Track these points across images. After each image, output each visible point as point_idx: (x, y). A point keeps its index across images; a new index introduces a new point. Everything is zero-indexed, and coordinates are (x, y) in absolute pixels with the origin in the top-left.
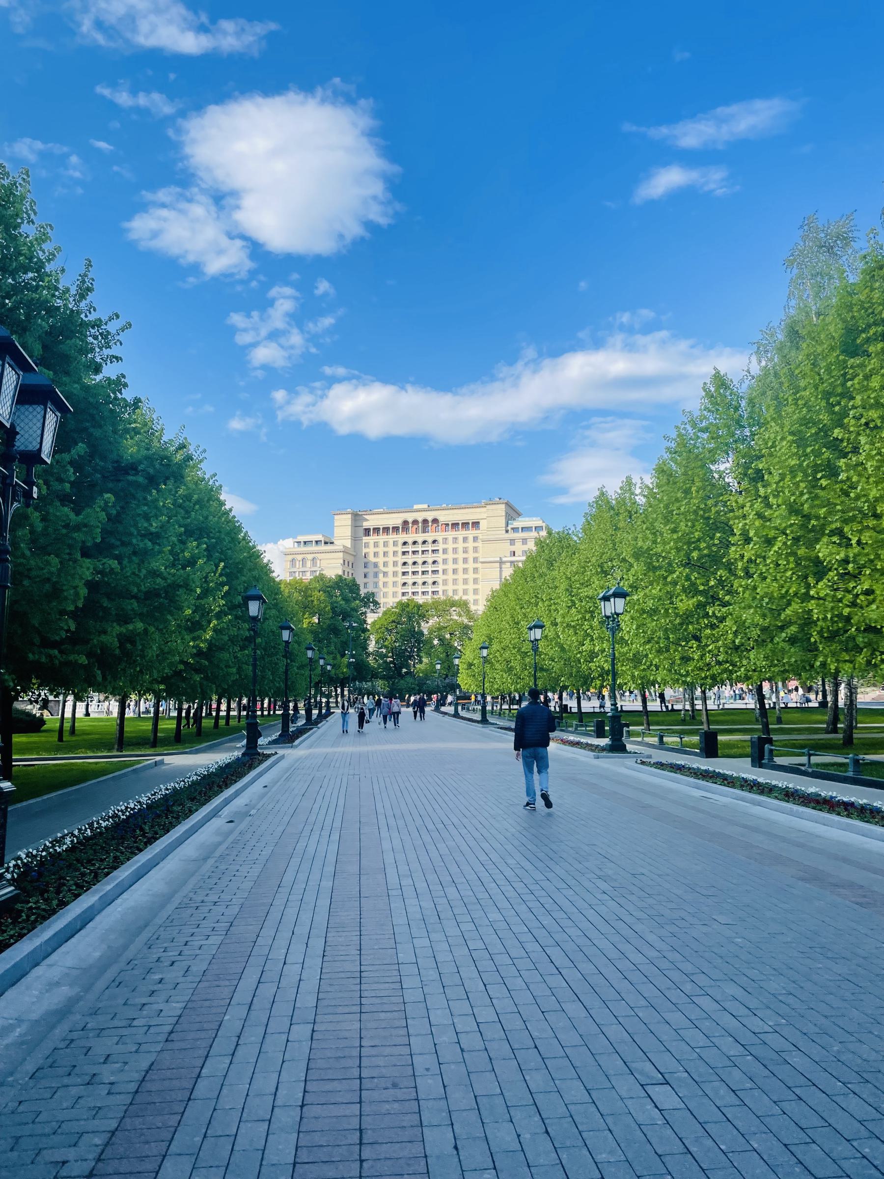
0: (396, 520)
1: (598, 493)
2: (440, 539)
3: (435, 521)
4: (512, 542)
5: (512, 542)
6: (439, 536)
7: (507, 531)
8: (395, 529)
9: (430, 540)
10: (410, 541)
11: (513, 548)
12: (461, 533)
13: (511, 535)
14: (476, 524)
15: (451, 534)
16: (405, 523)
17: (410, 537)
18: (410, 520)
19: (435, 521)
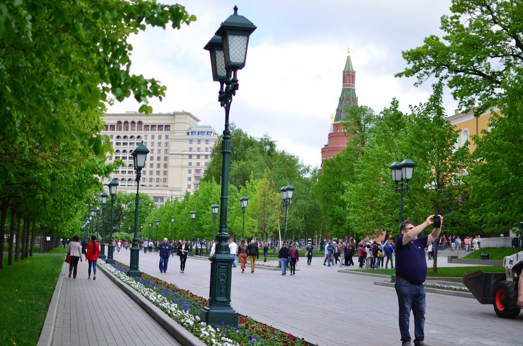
0: (114, 122)
1: (388, 106)
2: (143, 136)
3: (140, 123)
4: (191, 141)
5: (191, 141)
6: (142, 133)
7: (188, 134)
8: (112, 127)
9: (136, 136)
10: (122, 136)
11: (191, 146)
12: (156, 133)
13: (190, 137)
14: (167, 127)
15: (150, 133)
16: (119, 122)
17: (122, 133)
18: (123, 121)
19: (140, 123)
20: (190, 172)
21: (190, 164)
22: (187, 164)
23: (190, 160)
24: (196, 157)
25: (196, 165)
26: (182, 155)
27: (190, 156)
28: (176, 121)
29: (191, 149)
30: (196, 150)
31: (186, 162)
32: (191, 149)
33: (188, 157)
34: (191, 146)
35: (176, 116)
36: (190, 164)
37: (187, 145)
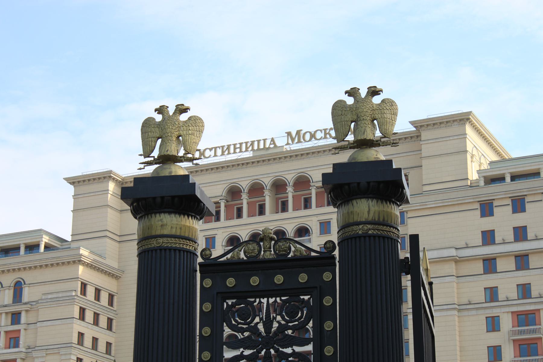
4: (487, 209)
11: (487, 223)
20: (493, 324)
21: (492, 294)
22: (480, 296)
23: (491, 280)
24: (510, 264)
25: (514, 294)
26: (457, 261)
27: (490, 265)
28: (427, 149)
29: (488, 237)
30: (510, 237)
31: (475, 290)
32: (488, 237)
33: (479, 267)
34: (487, 223)
35: (425, 135)
36: (492, 294)
37: (475, 223)
